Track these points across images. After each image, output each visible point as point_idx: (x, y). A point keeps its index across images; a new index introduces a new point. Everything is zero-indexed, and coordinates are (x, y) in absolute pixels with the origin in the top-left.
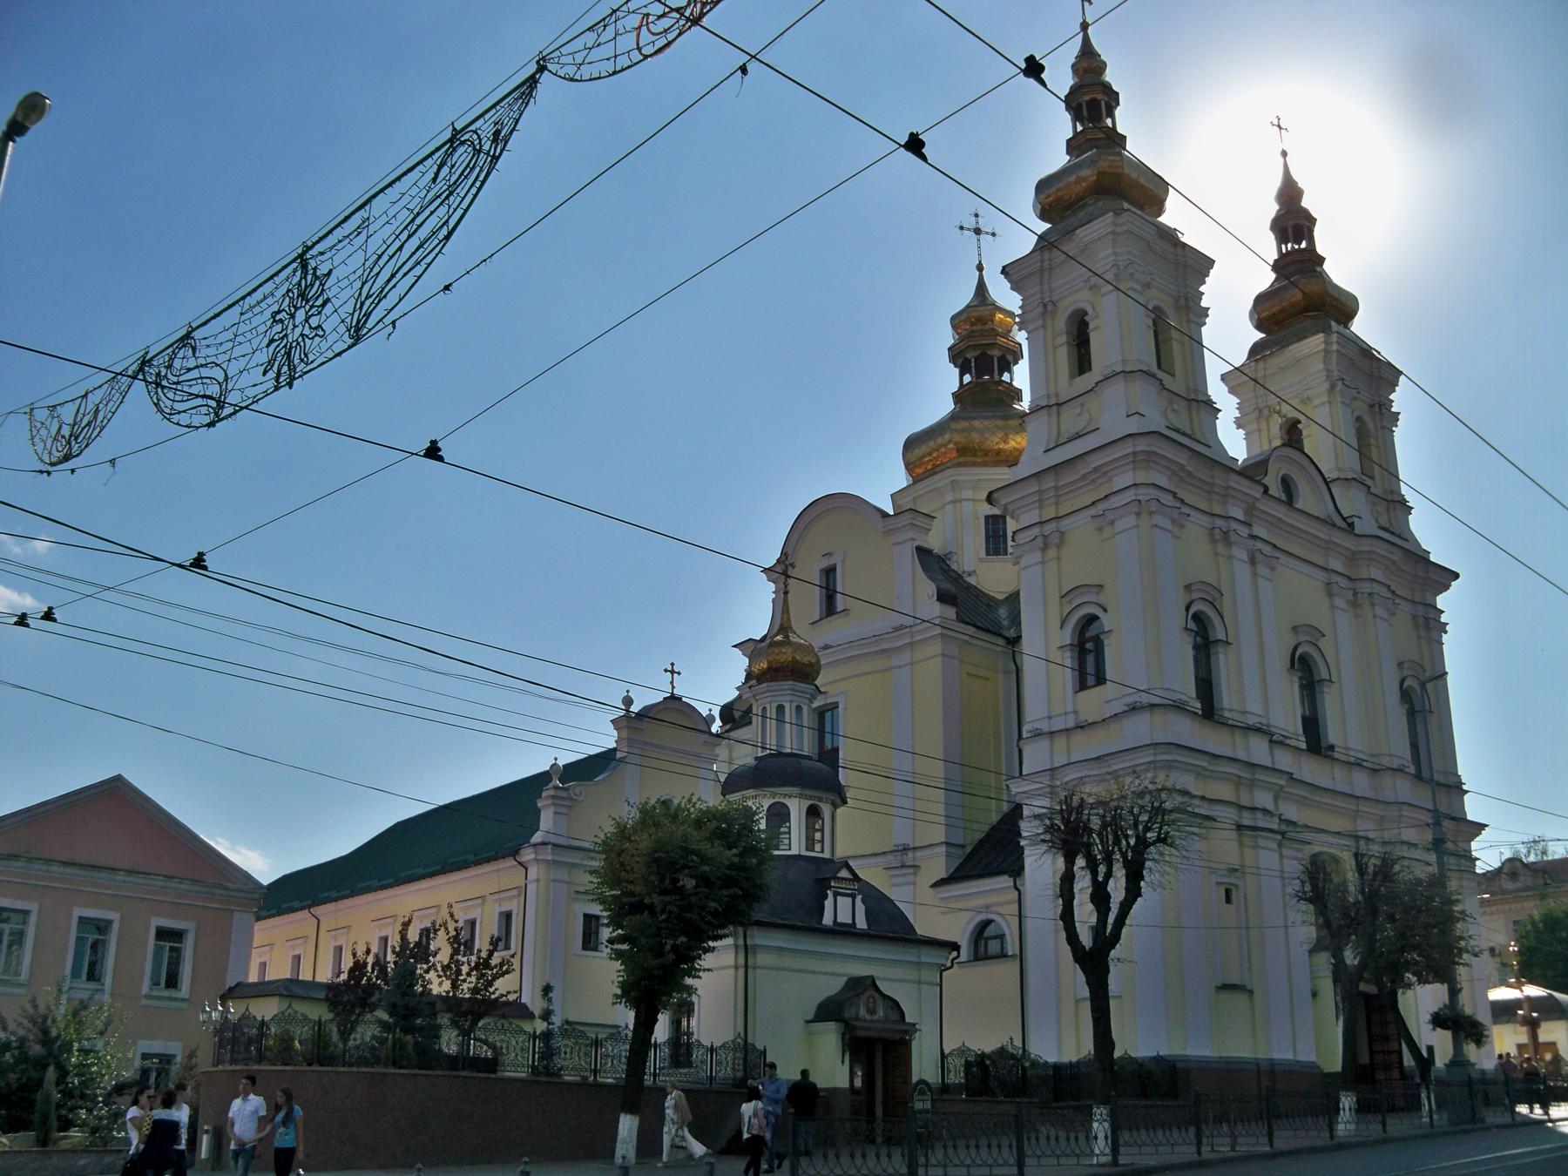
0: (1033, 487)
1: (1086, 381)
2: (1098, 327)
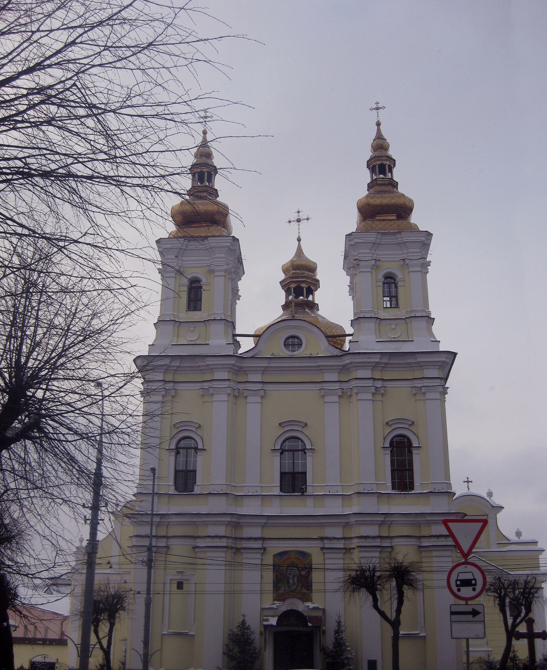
1: (196, 316)
2: (209, 290)
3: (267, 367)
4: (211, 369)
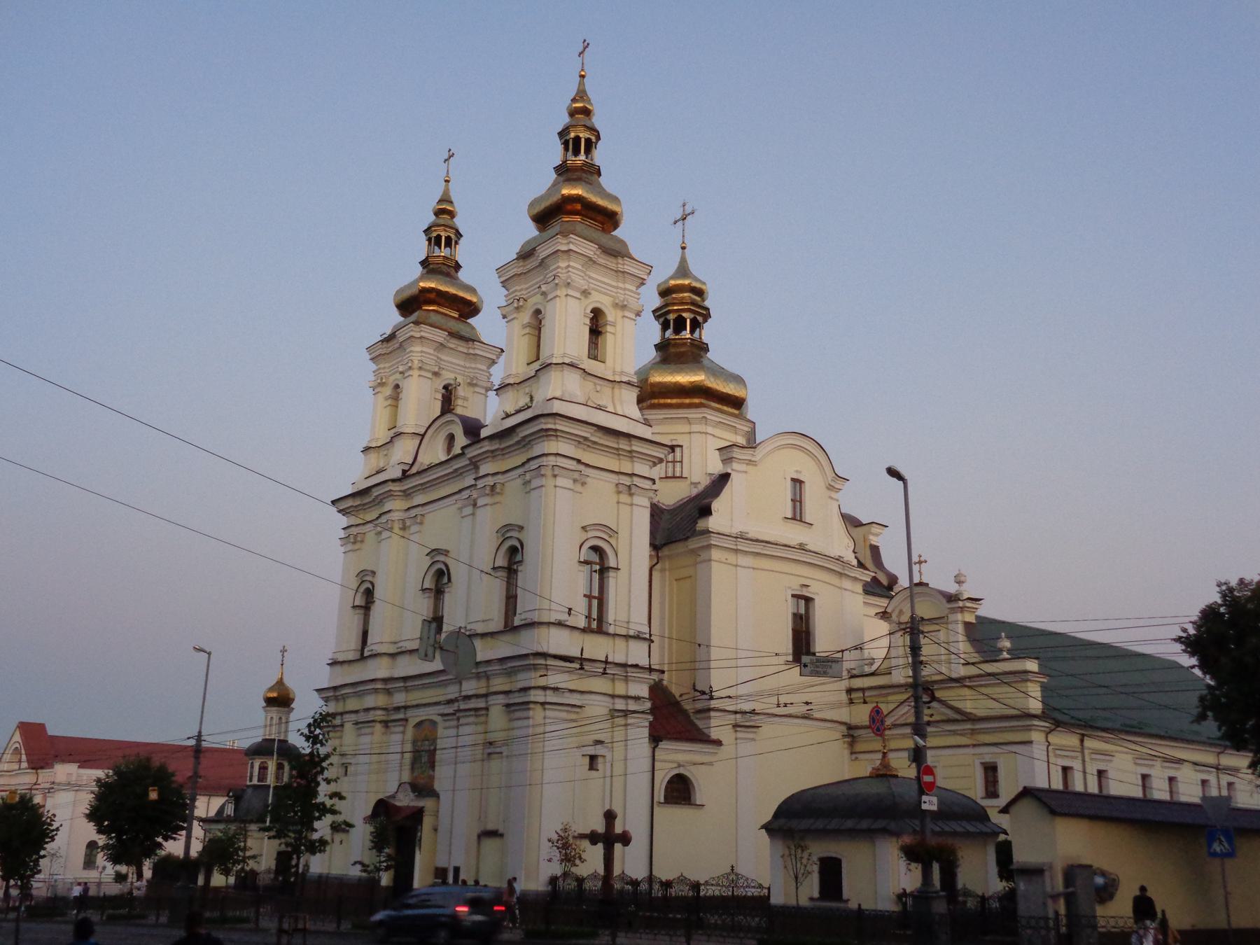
0: (349, 503)
3: (422, 484)
4: (379, 501)
